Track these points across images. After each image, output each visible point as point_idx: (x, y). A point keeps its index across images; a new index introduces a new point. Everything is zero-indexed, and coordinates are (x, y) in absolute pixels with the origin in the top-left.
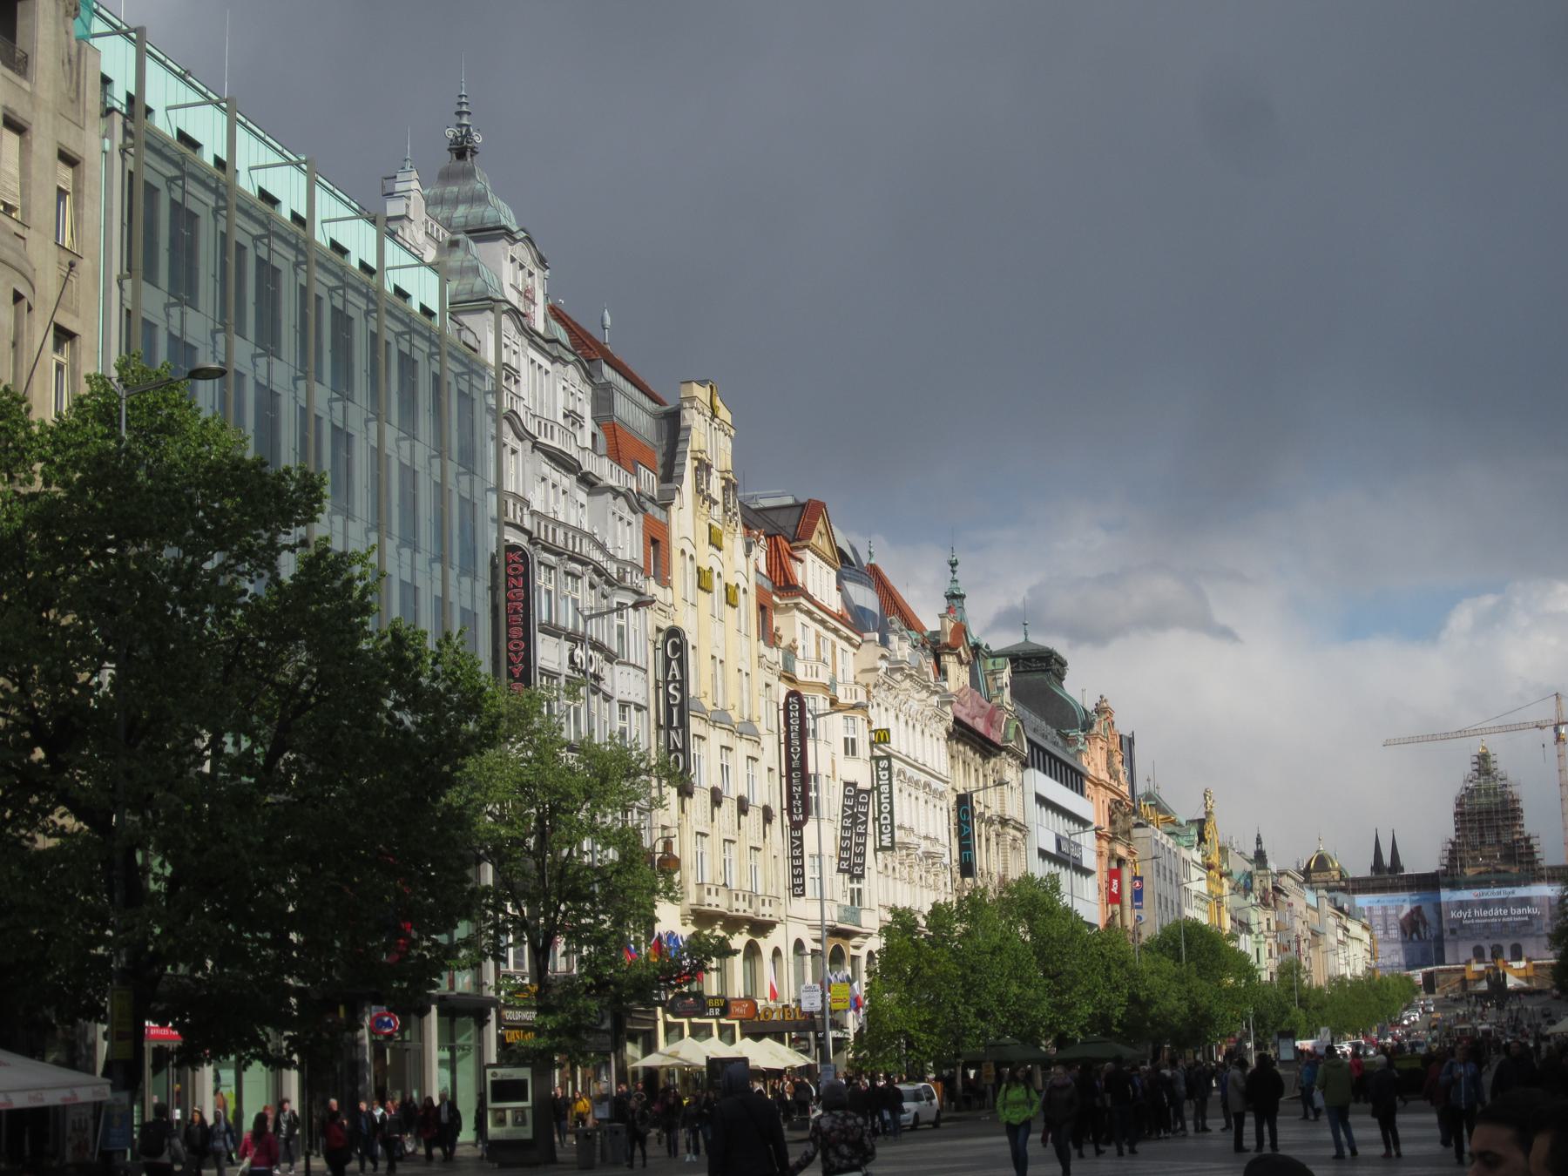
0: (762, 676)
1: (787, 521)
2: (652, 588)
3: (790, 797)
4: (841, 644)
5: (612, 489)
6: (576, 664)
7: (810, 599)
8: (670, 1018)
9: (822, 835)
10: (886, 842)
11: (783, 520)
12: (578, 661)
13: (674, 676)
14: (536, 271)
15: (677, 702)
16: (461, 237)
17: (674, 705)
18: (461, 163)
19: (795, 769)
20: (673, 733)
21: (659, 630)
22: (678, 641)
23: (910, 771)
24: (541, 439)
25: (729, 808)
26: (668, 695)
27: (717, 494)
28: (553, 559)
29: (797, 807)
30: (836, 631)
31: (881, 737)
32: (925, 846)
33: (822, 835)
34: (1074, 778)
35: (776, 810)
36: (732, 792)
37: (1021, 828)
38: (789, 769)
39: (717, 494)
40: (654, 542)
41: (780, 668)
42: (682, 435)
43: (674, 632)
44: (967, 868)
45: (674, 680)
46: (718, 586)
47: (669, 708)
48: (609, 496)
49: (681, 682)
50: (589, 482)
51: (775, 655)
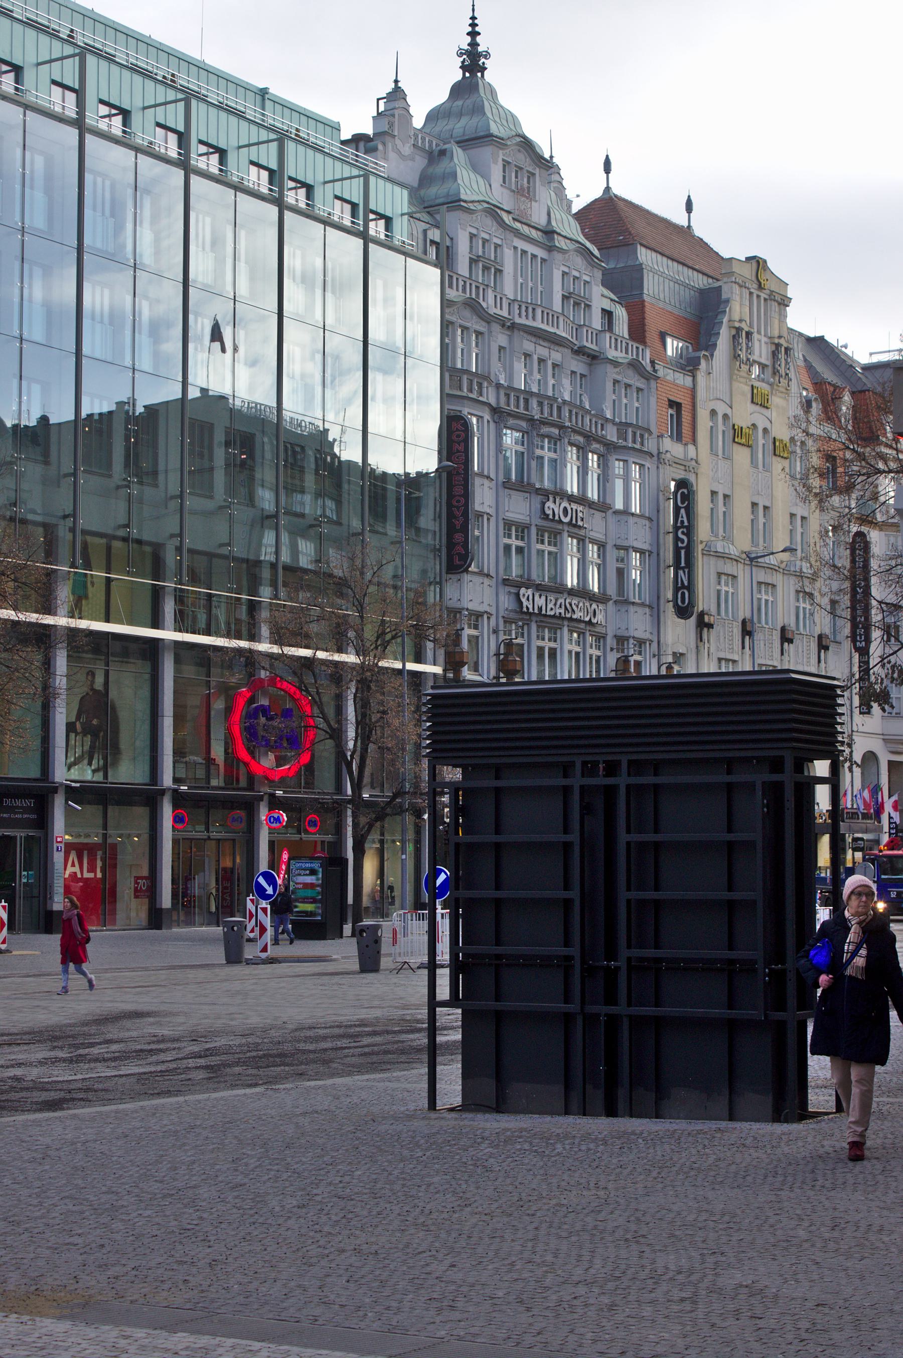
2: (668, 444)
6: (548, 515)
12: (550, 512)
13: (682, 522)
15: (685, 544)
17: (682, 548)
19: (860, 601)
20: (681, 572)
22: (685, 491)
24: (523, 321)
26: (677, 539)
29: (860, 635)
40: (675, 405)
45: (682, 526)
47: (677, 551)
49: (688, 528)
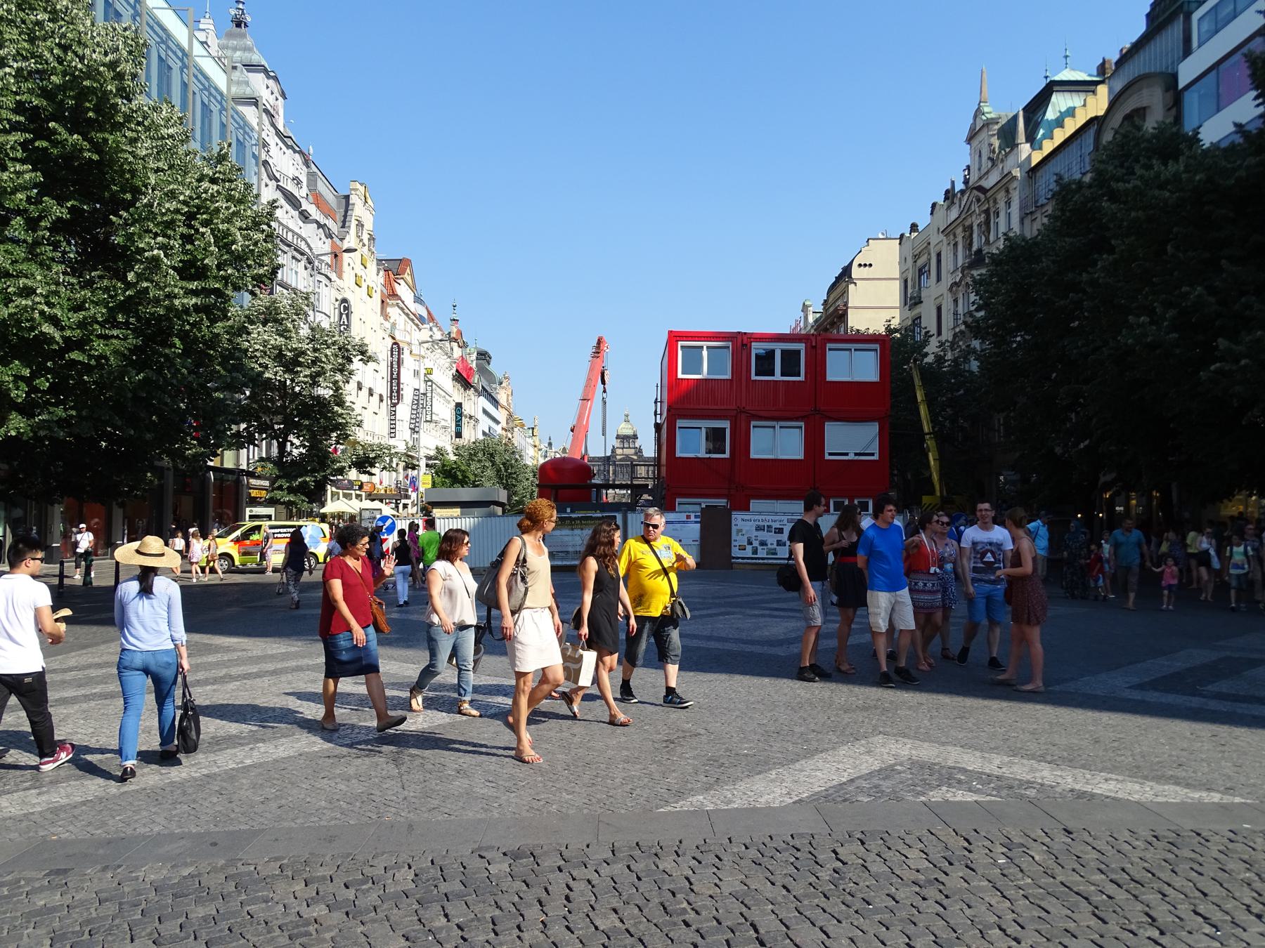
0: (381, 334)
1: (394, 266)
2: (333, 276)
3: (392, 391)
4: (415, 327)
5: (317, 222)
7: (403, 302)
8: (334, 489)
9: (404, 411)
10: (429, 419)
11: (391, 265)
14: (280, 98)
16: (238, 65)
18: (239, 29)
21: (337, 300)
23: (438, 390)
25: (365, 392)
27: (366, 241)
28: (286, 249)
30: (412, 320)
31: (429, 372)
32: (443, 423)
33: (404, 411)
34: (495, 402)
35: (385, 398)
36: (366, 385)
37: (477, 421)
38: (392, 379)
39: (366, 241)
41: (389, 331)
42: (350, 207)
43: (345, 301)
44: (459, 435)
46: (364, 286)
48: (315, 225)
50: (305, 216)
51: (388, 325)
